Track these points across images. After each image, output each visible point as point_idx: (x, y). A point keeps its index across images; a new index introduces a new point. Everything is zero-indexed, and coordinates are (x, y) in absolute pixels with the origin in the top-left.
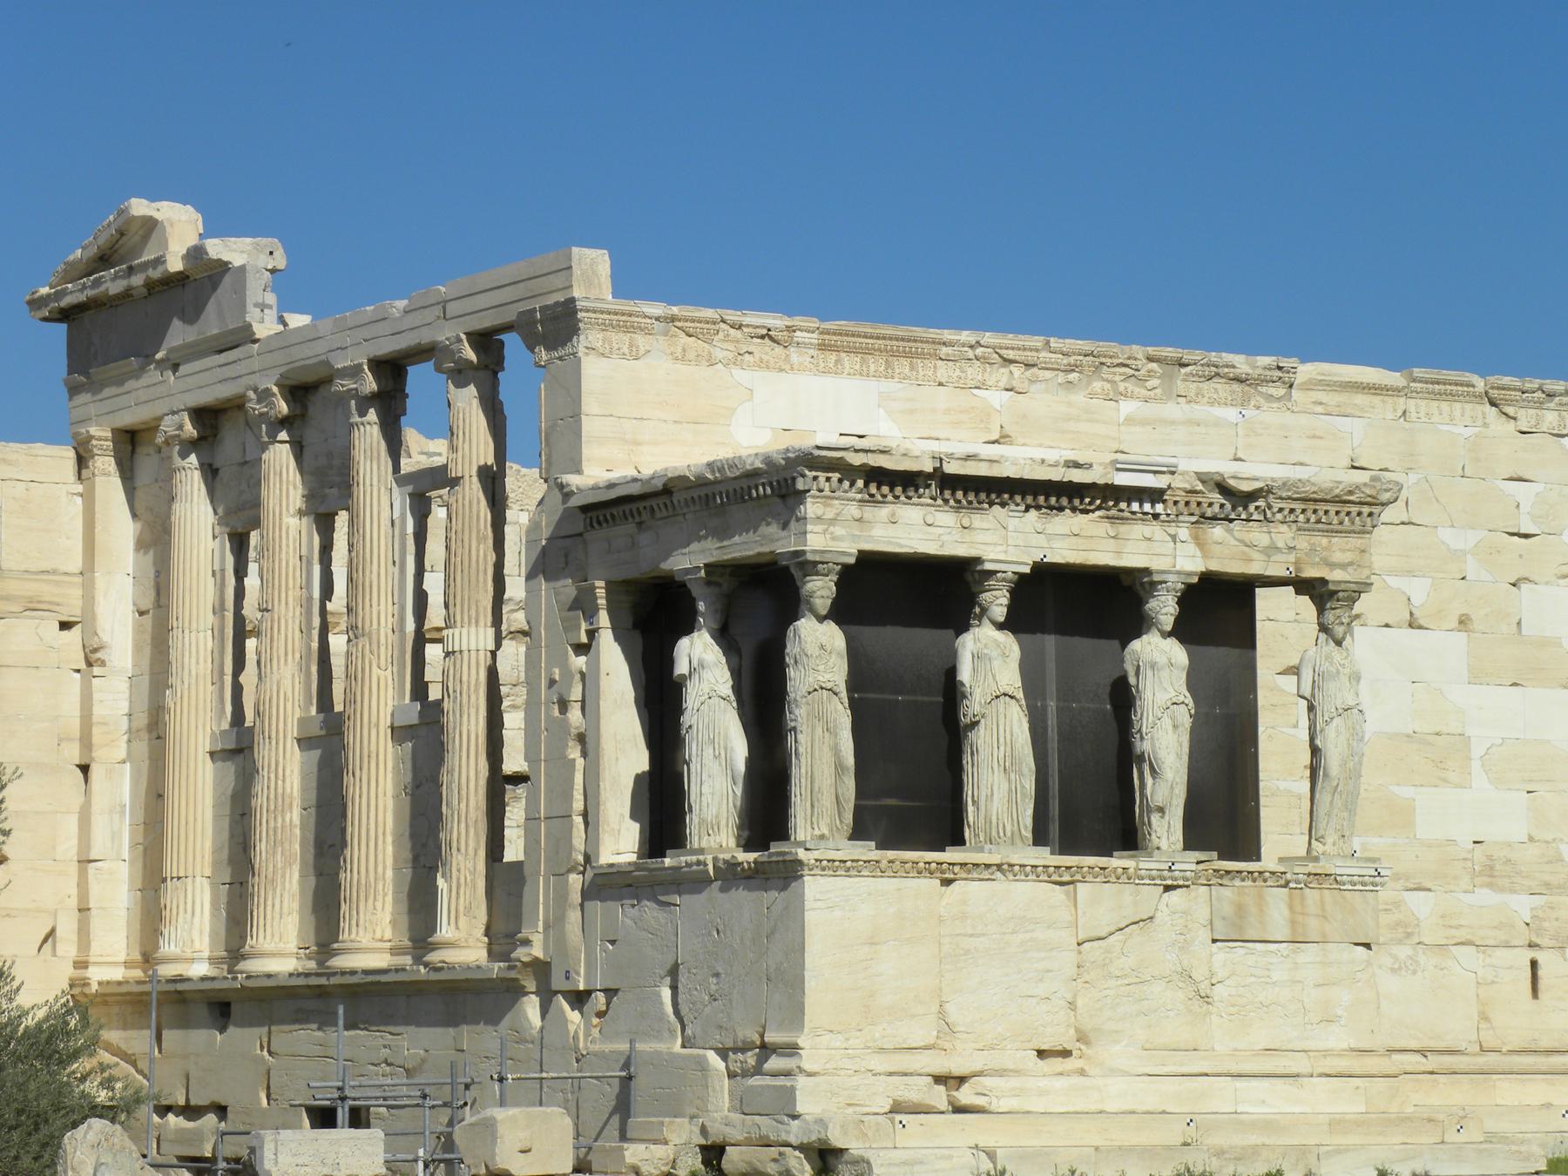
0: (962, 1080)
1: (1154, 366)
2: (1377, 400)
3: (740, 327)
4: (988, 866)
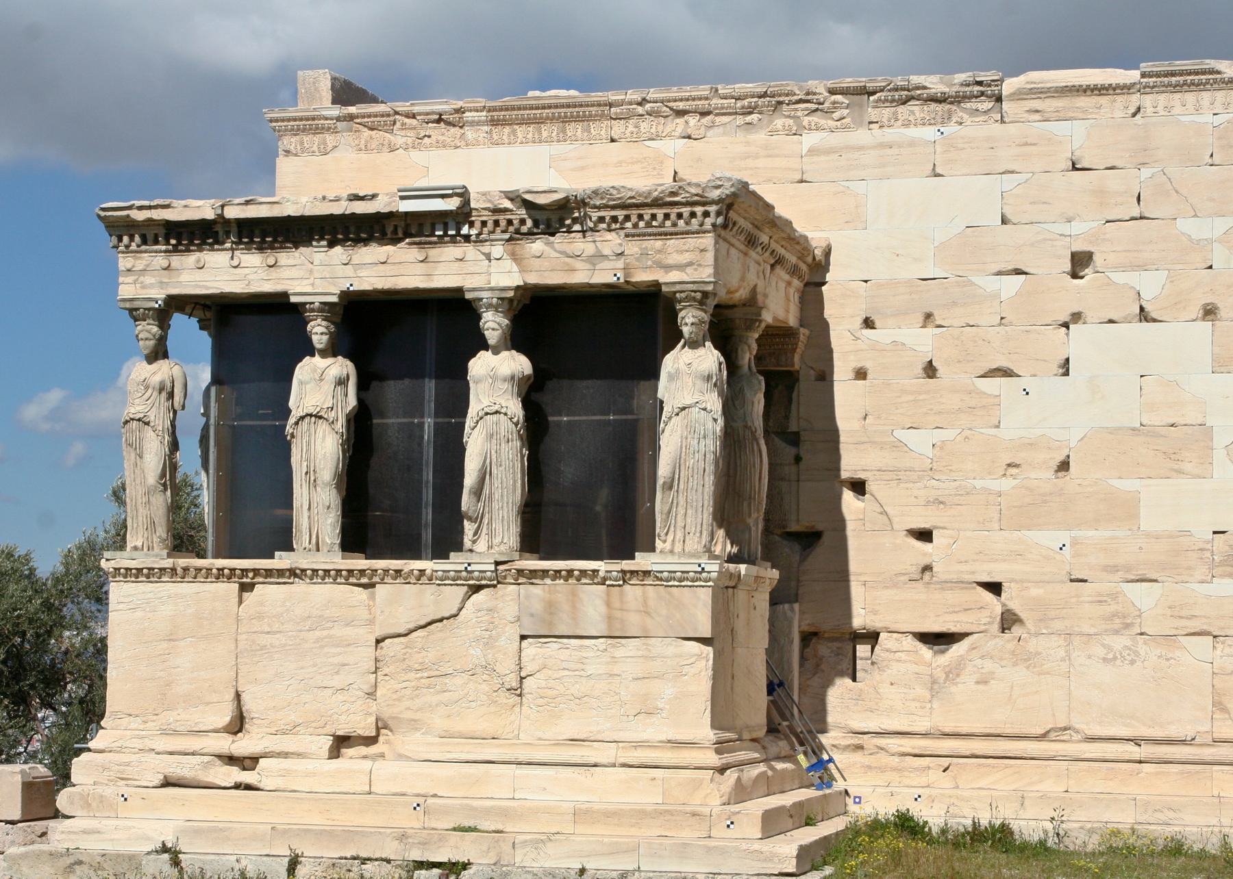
1: (839, 98)
2: (1104, 100)
3: (414, 117)
4: (281, 573)
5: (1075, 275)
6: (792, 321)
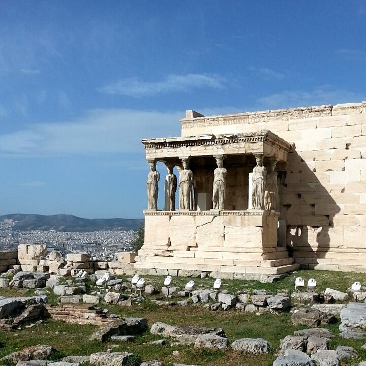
0: (173, 251)
1: (296, 112)
4: (177, 213)
5: (347, 149)
6: (285, 161)
